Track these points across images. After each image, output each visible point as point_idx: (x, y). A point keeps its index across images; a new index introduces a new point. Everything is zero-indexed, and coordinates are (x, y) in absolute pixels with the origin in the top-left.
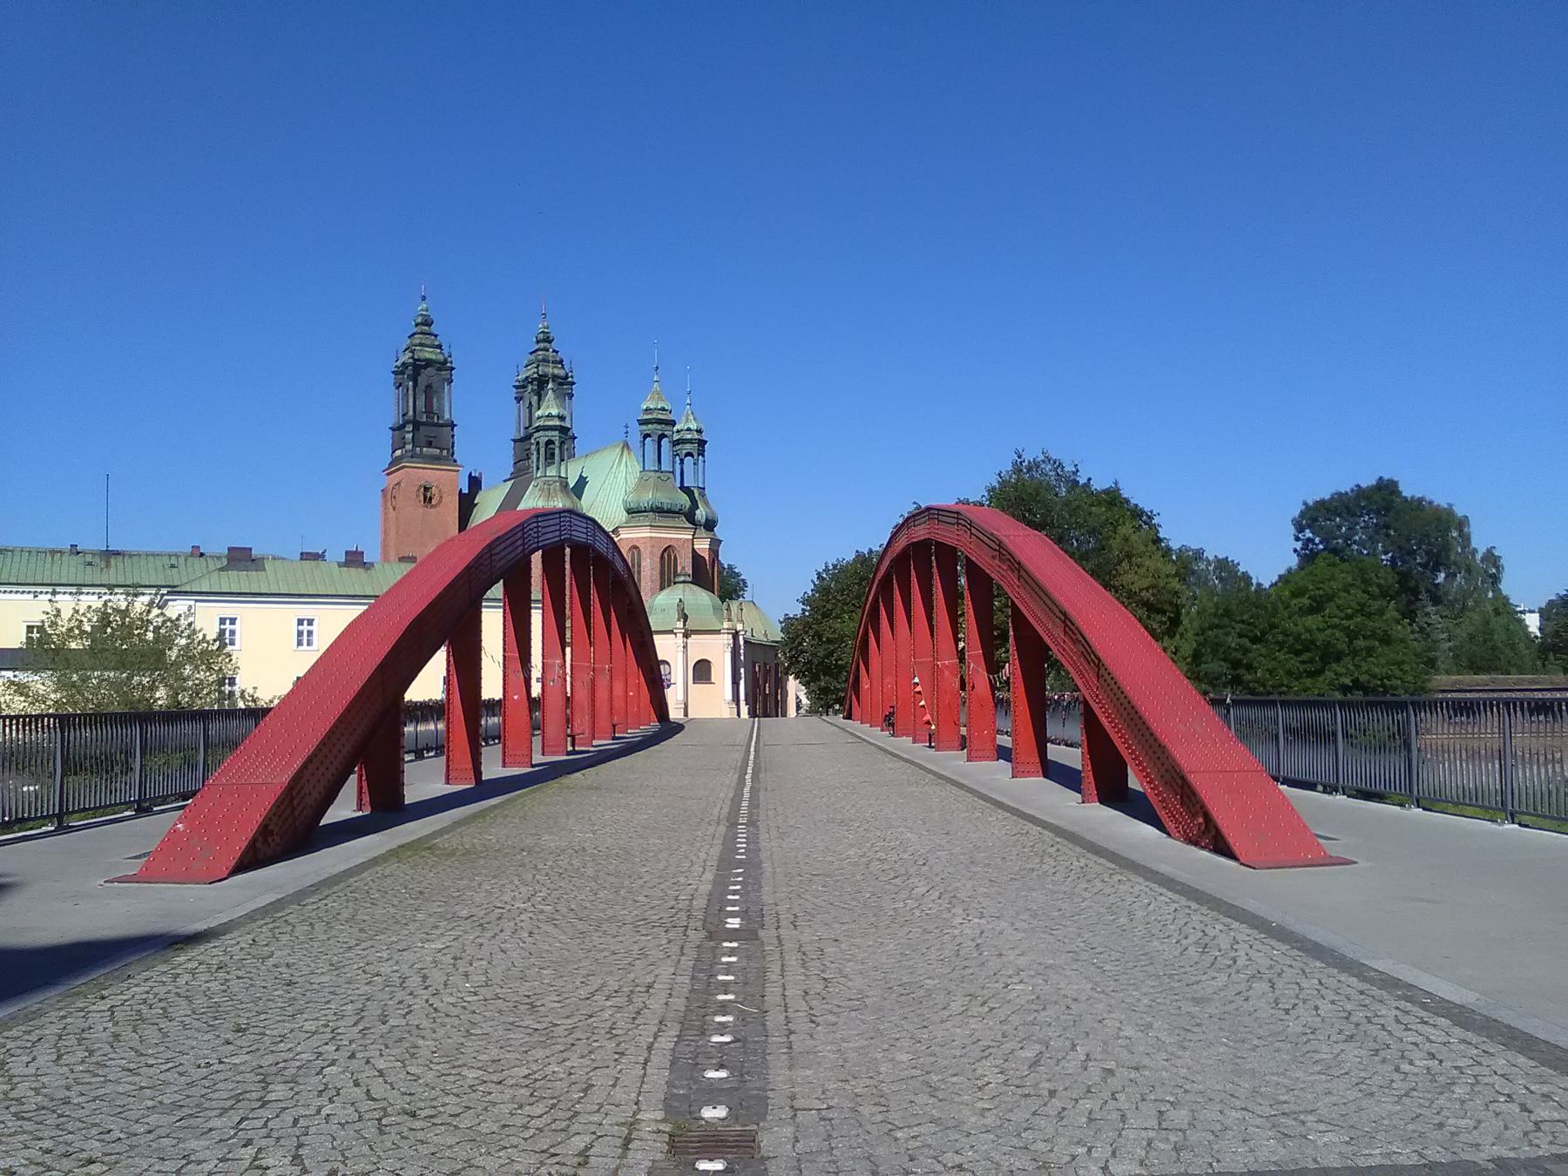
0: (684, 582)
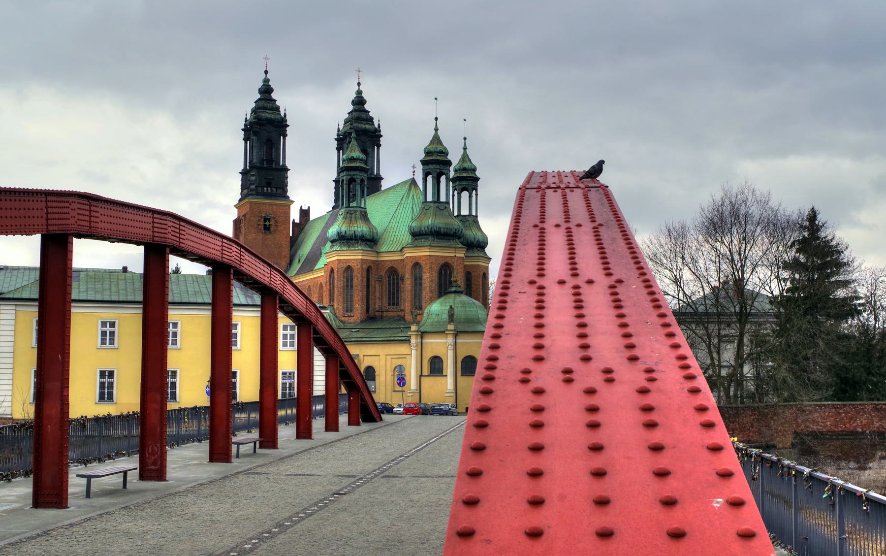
0: (455, 292)
